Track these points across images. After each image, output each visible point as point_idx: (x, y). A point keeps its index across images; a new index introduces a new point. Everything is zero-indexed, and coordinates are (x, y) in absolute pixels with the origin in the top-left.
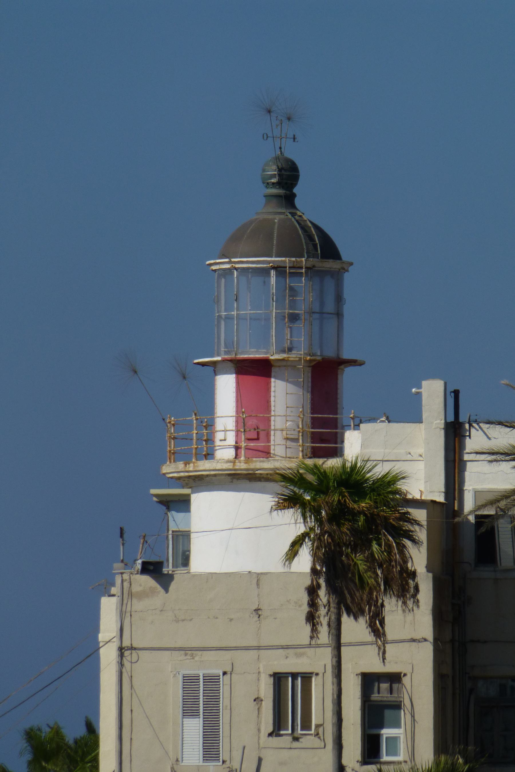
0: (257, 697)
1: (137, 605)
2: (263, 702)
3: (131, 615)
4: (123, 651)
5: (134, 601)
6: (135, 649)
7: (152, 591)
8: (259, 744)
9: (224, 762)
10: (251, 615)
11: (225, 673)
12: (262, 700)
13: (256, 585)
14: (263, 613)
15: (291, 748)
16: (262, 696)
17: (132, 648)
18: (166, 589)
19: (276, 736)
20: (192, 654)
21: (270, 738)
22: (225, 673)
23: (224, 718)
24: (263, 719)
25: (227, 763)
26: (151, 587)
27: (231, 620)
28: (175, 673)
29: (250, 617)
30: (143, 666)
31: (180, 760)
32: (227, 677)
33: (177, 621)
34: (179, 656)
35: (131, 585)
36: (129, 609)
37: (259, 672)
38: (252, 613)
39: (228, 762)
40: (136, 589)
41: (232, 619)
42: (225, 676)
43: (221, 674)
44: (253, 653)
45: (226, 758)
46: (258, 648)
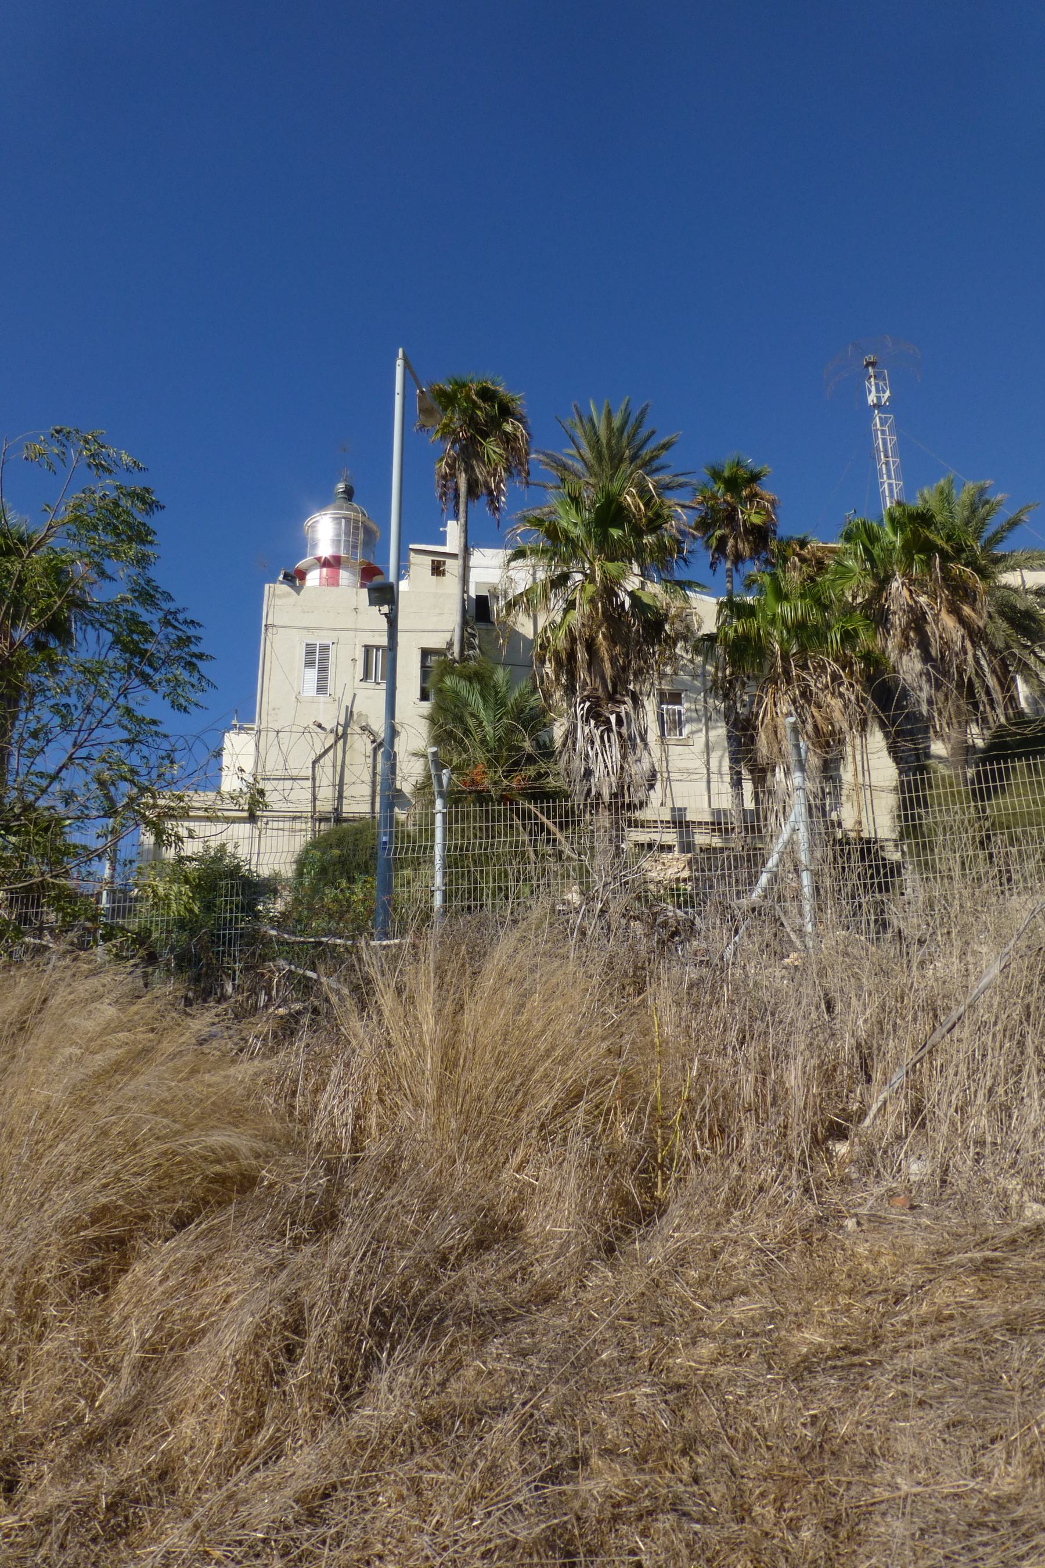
1: (278, 602)
7: (289, 594)
17: (274, 626)
23: (331, 668)
46: (356, 630)
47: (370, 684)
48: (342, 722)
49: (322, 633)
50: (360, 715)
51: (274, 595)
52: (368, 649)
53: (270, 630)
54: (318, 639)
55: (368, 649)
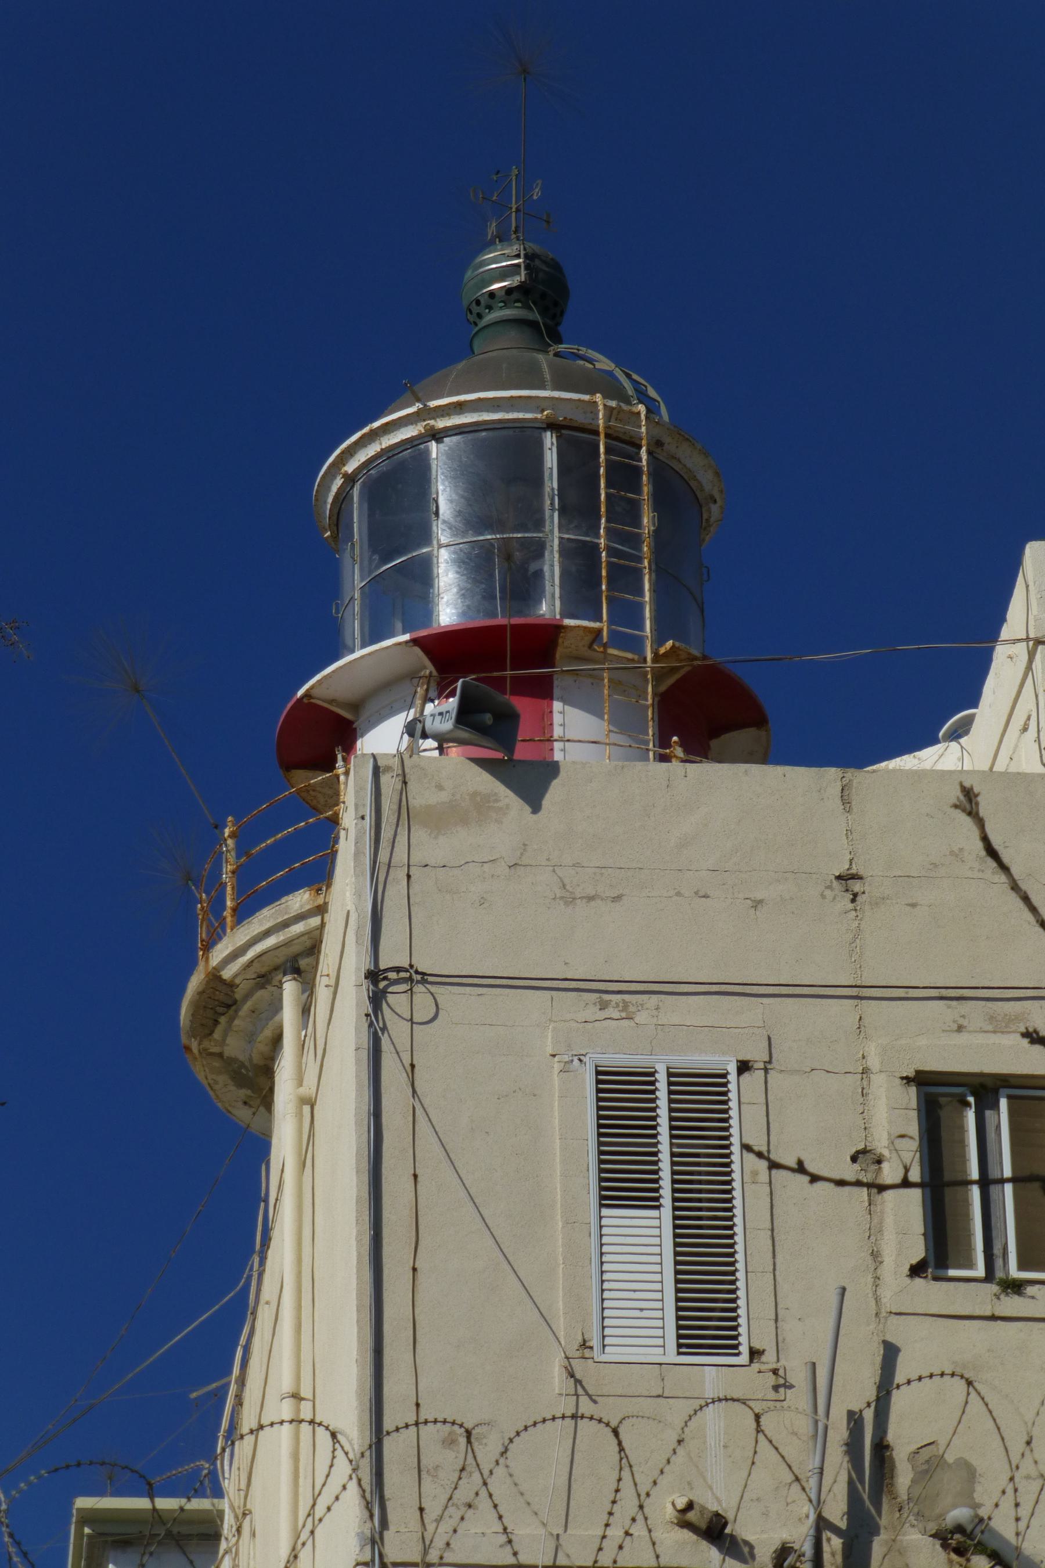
0: (861, 1146)
1: (428, 847)
2: (885, 1165)
3: (409, 876)
4: (382, 984)
5: (419, 834)
6: (424, 978)
8: (877, 1300)
9: (755, 1354)
10: (828, 893)
11: (744, 1067)
12: (879, 1162)
13: (839, 802)
14: (867, 889)
15: (993, 1318)
16: (880, 1143)
17: (414, 977)
18: (534, 799)
19: (936, 1279)
20: (626, 1005)
21: (918, 1281)
22: (744, 1067)
24: (889, 1221)
25: (764, 1358)
26: (475, 794)
27: (757, 904)
28: (566, 1058)
29: (823, 896)
30: (451, 1039)
31: (595, 1343)
32: (753, 1080)
33: (570, 900)
34: (580, 1008)
35: (405, 783)
36: (400, 855)
37: (865, 1071)
38: (829, 887)
39: (770, 1357)
40: (421, 796)
41: (761, 902)
42: (746, 1076)
43: (732, 1068)
44: (843, 1011)
45: (764, 1341)
46: (858, 993)
47: (965, 1292)
48: (836, 1511)
49: (680, 1011)
50: (931, 1464)
51: (404, 812)
52: (939, 1096)
53: (397, 1000)
54: (667, 1043)
55: (939, 1096)
